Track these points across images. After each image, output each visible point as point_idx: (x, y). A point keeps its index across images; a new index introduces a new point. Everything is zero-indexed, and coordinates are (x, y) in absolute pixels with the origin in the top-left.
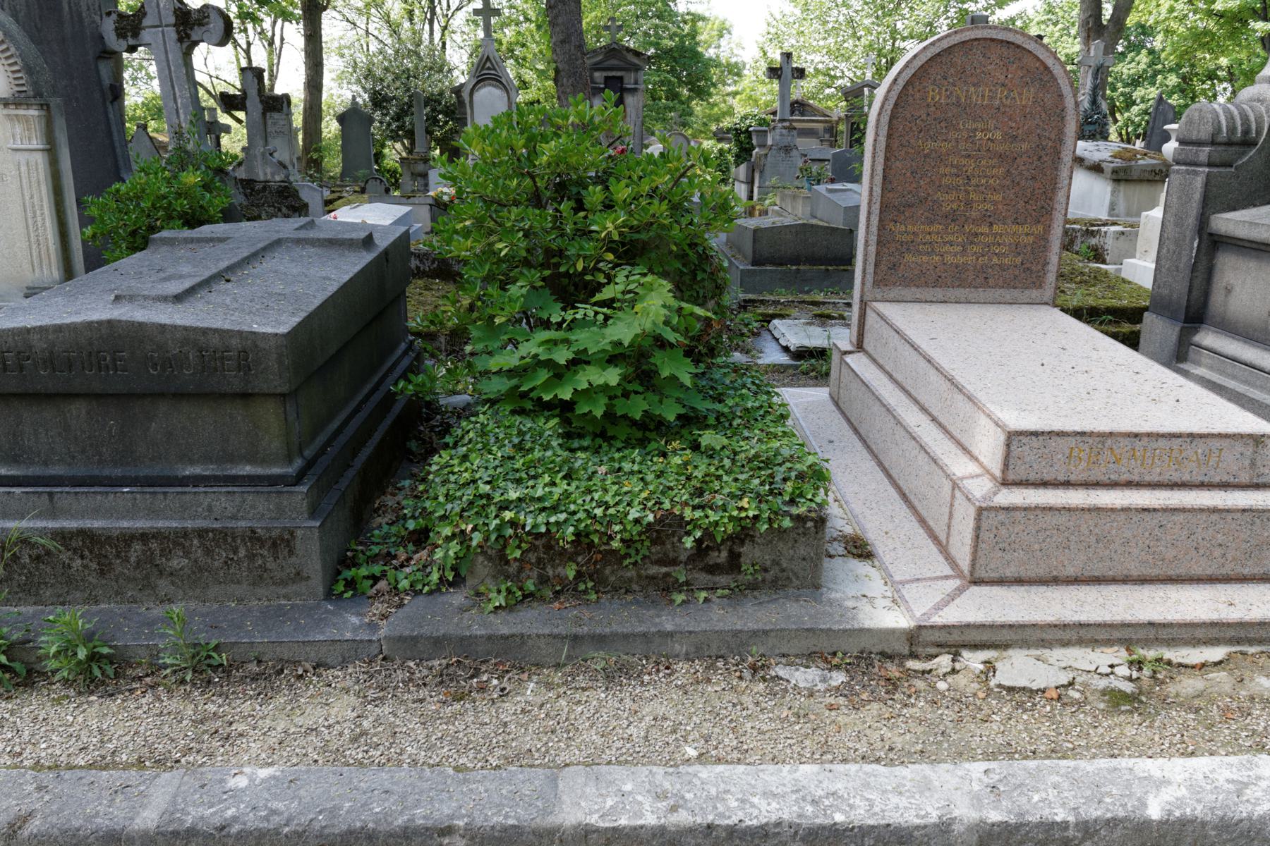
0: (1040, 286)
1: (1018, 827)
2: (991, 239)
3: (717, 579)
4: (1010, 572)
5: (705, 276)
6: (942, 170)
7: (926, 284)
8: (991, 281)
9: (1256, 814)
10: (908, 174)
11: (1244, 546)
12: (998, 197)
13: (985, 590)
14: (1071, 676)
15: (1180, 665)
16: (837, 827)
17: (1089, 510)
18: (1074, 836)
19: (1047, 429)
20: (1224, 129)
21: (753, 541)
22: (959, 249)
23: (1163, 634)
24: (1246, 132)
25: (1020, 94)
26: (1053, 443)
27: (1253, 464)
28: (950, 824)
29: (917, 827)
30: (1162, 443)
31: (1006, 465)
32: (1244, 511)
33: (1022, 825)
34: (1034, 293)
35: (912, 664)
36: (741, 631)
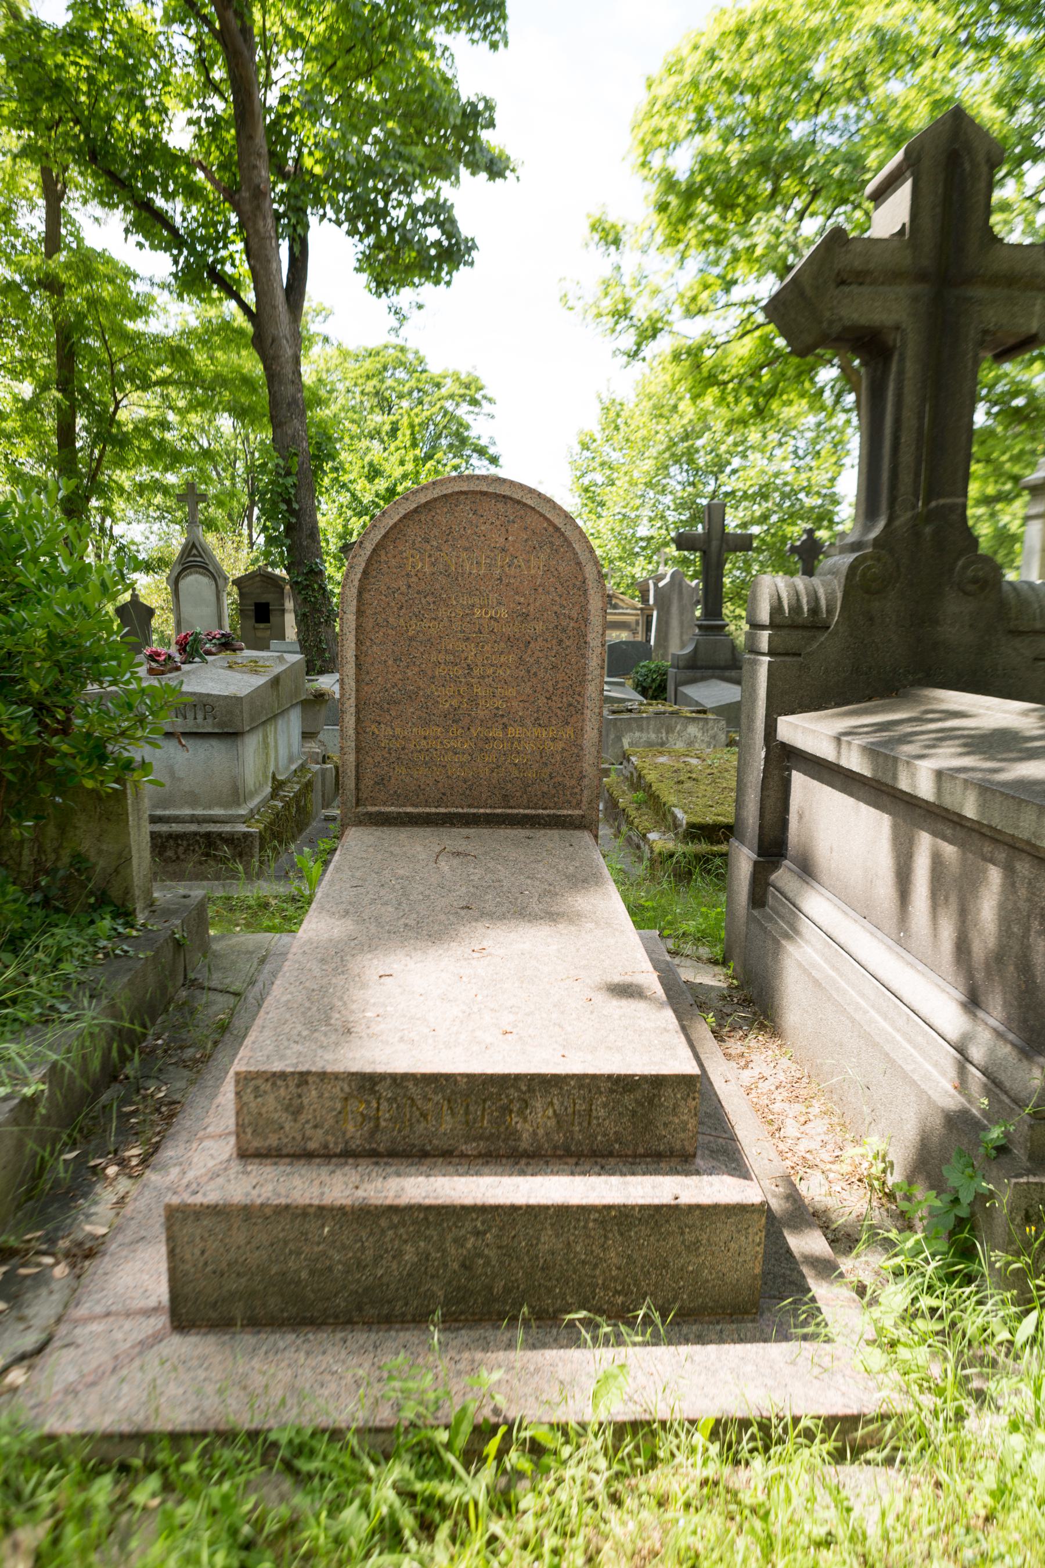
2: (507, 746)
10: (390, 662)
12: (511, 692)
22: (466, 758)
24: (815, 610)
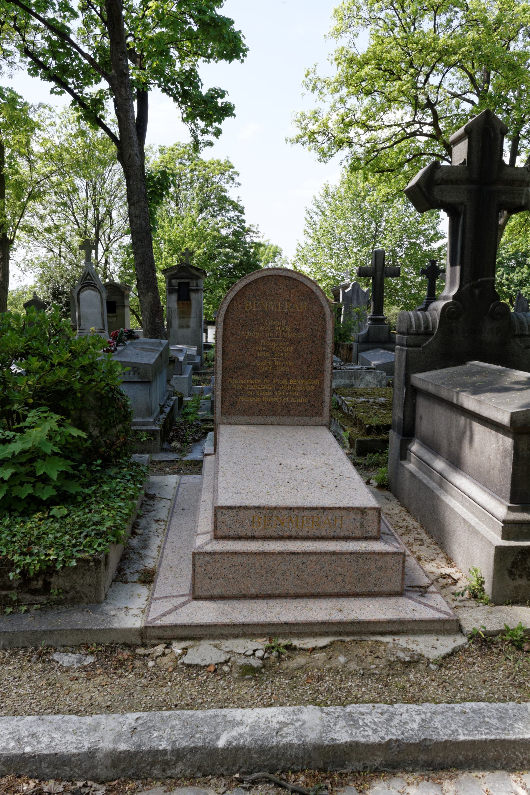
0: (321, 415)
1: (136, 753)
2: (289, 388)
3: (37, 598)
4: (216, 592)
5: (113, 410)
6: (257, 348)
7: (253, 414)
8: (292, 412)
9: (281, 743)
10: (238, 350)
11: (355, 574)
12: (291, 364)
13: (200, 603)
14: (229, 657)
15: (301, 649)
16: (25, 755)
17: (259, 554)
18: (171, 759)
19: (238, 505)
20: (414, 326)
21: (58, 575)
22: (271, 393)
23: (294, 630)
24: (427, 327)
25: (299, 306)
26: (242, 513)
27: (362, 525)
28: (95, 753)
29: (74, 755)
30: (306, 513)
31: (215, 527)
32: (351, 553)
33: (138, 752)
34: (317, 419)
35: (140, 651)
36: (36, 631)
